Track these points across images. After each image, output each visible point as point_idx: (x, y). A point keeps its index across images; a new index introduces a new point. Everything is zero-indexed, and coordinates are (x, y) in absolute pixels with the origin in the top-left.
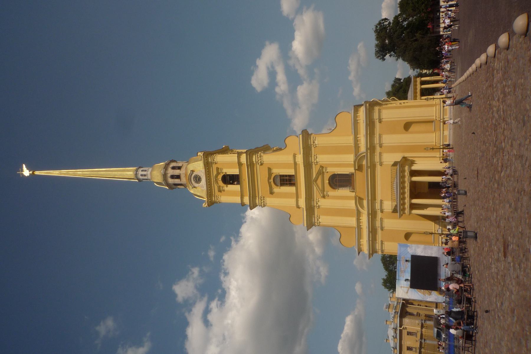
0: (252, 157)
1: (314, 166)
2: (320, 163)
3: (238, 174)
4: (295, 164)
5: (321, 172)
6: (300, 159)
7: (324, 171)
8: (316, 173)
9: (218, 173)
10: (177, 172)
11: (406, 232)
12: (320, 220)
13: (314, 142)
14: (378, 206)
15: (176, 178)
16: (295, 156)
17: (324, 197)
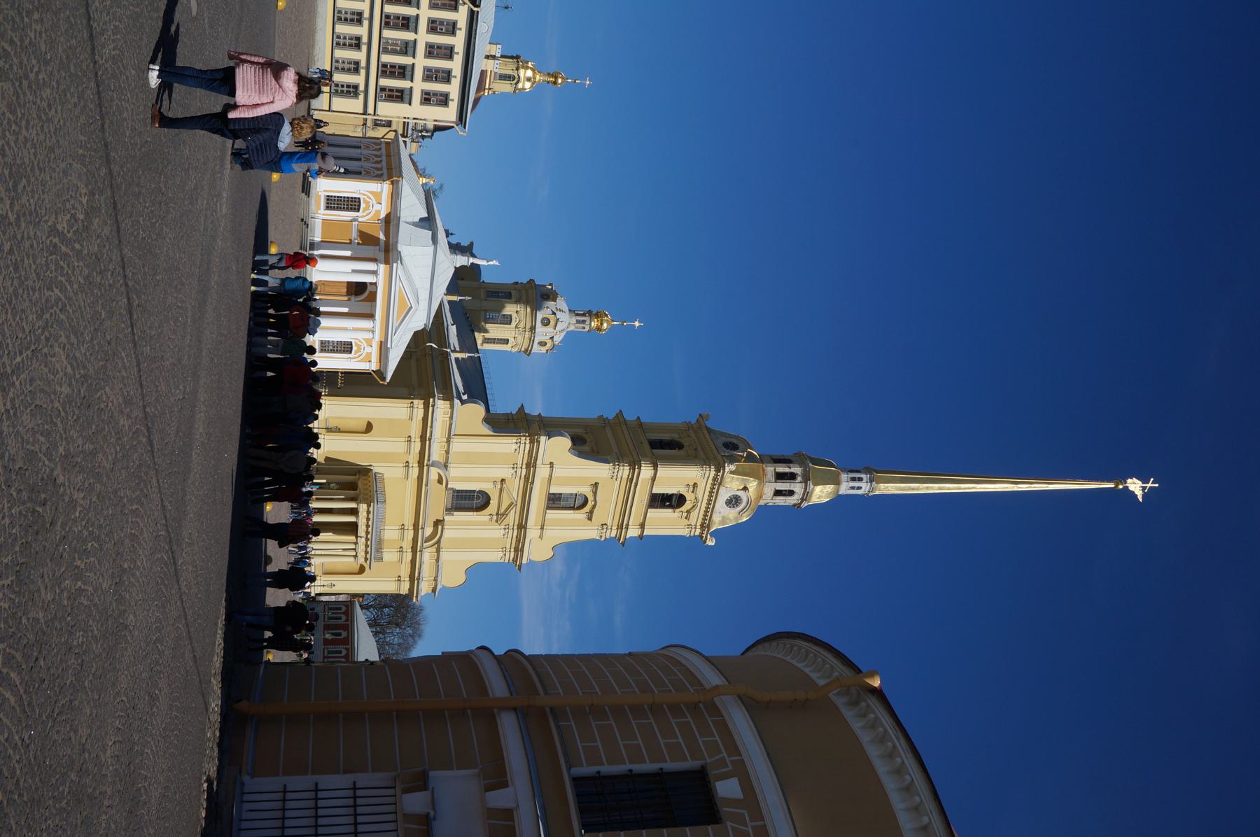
0: (616, 535)
1: (511, 524)
2: (500, 527)
3: (649, 510)
4: (542, 528)
5: (501, 516)
6: (532, 533)
7: (495, 517)
8: (507, 518)
9: (688, 512)
10: (780, 501)
11: (370, 433)
12: (516, 446)
13: (505, 555)
14: (415, 472)
15: (786, 491)
16: (541, 537)
17: (503, 480)
